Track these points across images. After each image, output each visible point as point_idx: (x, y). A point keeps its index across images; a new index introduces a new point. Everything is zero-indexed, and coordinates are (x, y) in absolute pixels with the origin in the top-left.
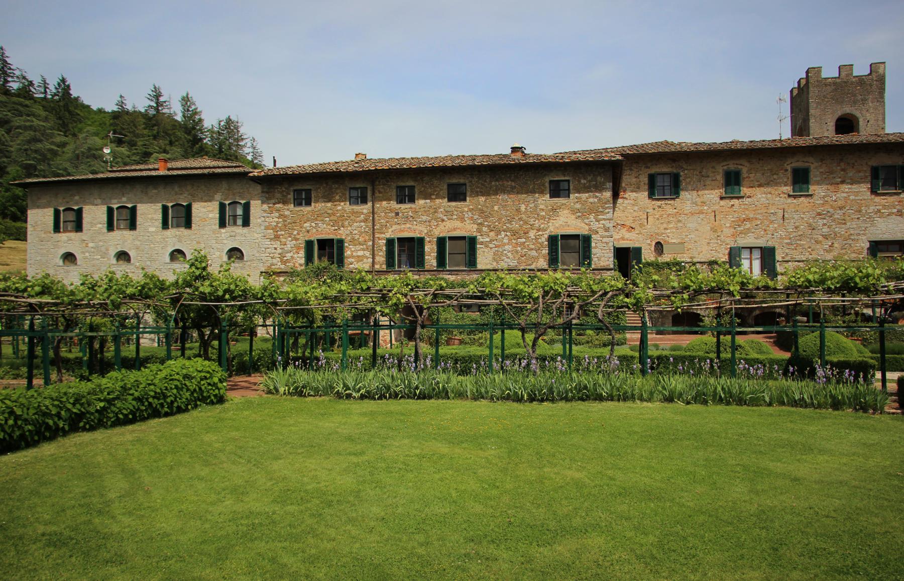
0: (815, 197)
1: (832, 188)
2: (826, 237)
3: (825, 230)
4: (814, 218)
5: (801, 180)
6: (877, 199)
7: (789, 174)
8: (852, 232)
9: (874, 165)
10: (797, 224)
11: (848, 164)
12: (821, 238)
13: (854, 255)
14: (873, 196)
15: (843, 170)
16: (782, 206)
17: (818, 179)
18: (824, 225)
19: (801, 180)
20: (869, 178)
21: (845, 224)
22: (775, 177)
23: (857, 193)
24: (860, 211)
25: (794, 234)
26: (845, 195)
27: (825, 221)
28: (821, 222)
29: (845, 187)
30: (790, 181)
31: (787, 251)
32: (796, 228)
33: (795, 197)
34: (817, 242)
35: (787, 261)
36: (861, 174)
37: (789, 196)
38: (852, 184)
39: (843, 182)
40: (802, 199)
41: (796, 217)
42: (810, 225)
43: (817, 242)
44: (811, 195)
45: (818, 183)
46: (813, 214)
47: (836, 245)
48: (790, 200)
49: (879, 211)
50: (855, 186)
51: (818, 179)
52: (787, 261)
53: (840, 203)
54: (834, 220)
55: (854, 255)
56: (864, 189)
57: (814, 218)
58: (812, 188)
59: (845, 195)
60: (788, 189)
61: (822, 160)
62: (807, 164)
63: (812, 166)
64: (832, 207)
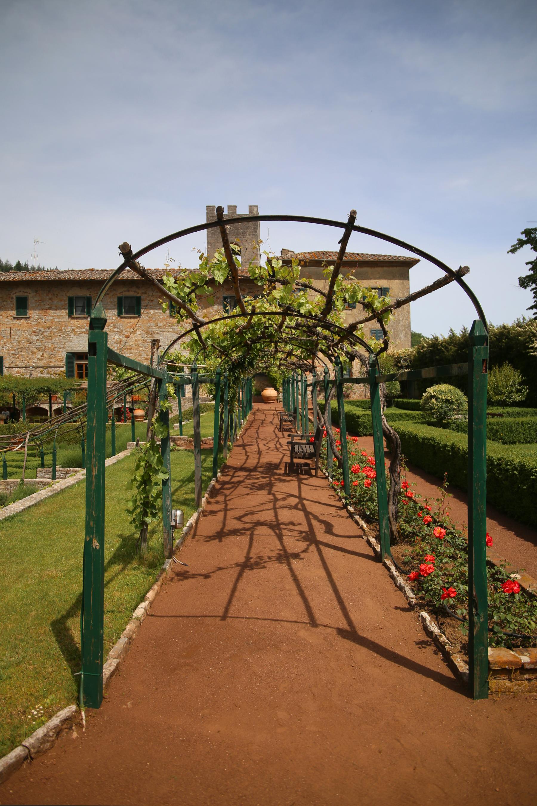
0: (32, 319)
1: (42, 312)
2: (38, 349)
3: (38, 344)
4: (31, 335)
5: (22, 306)
6: (73, 321)
7: (14, 301)
8: (56, 346)
9: (71, 295)
10: (20, 339)
11: (54, 294)
12: (35, 350)
13: (57, 363)
14: (70, 319)
15: (50, 299)
16: (9, 326)
17: (34, 305)
18: (38, 340)
19: (22, 306)
20: (67, 306)
21: (51, 339)
22: (5, 303)
23: (59, 317)
24: (61, 330)
25: (18, 347)
26: (51, 318)
27: (38, 337)
28: (35, 338)
29: (52, 312)
30: (15, 307)
31: (13, 359)
32: (19, 342)
33: (18, 319)
34: (33, 353)
35: (12, 368)
36: (63, 303)
37: (14, 318)
38: (56, 310)
39: (50, 308)
40: (23, 320)
41: (19, 334)
42: (28, 340)
43: (33, 353)
44: (29, 318)
45: (34, 309)
46: (30, 332)
47: (45, 355)
48: (15, 321)
49: (74, 330)
50: (58, 312)
51: (34, 305)
52: (12, 368)
53: (48, 324)
54: (44, 337)
55: (57, 363)
56: (64, 313)
57: (31, 335)
58: (30, 312)
59: (51, 318)
60: (14, 313)
61: (36, 291)
62: (26, 294)
63: (30, 296)
64: (43, 327)
